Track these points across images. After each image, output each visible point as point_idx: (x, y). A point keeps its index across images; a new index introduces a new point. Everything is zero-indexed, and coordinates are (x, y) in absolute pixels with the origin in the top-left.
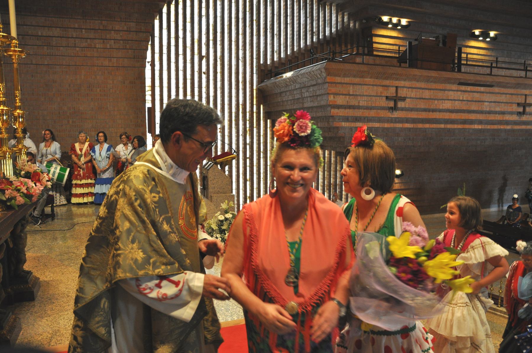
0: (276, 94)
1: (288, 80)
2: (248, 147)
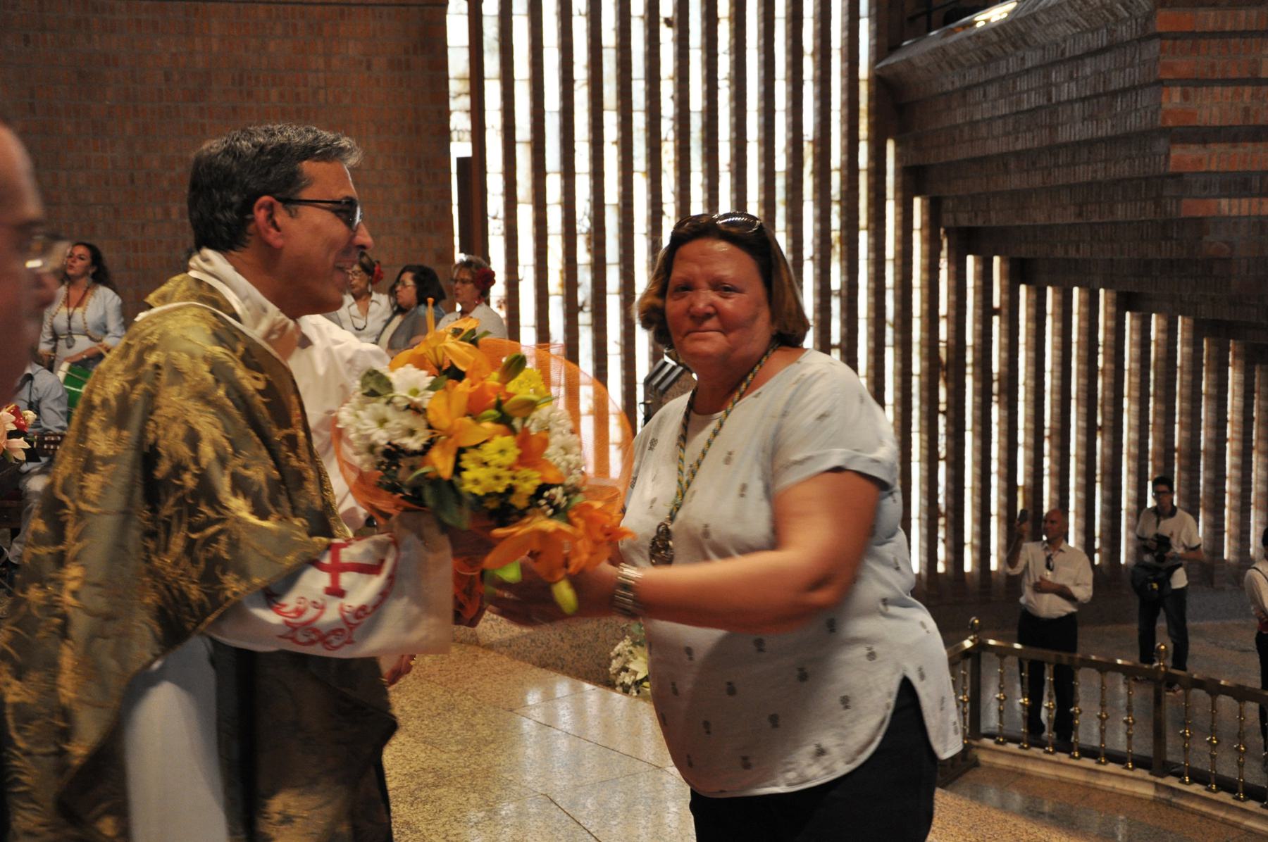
0: (947, 94)
1: (994, 38)
2: (836, 304)
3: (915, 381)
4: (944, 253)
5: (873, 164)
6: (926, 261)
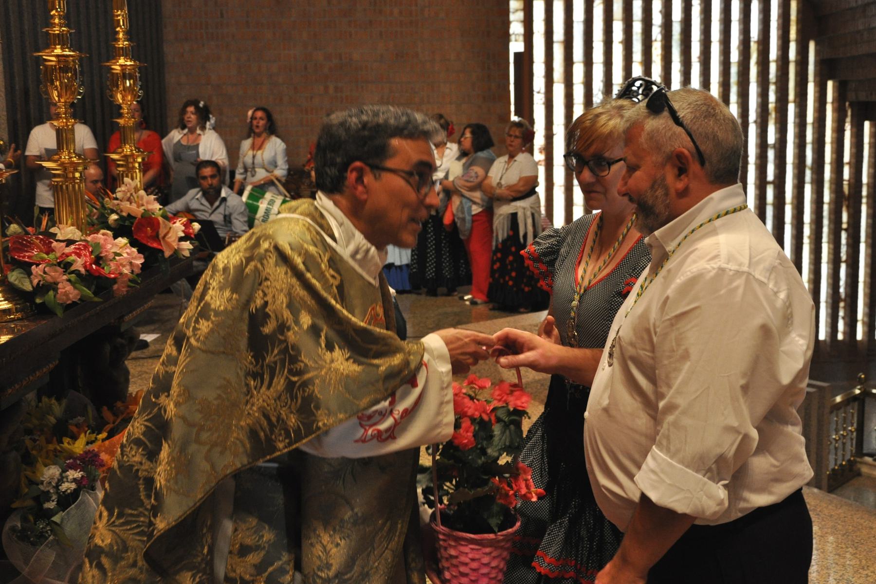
2: (771, 154)
3: (826, 208)
4: (848, 119)
5: (799, 58)
6: (835, 125)
